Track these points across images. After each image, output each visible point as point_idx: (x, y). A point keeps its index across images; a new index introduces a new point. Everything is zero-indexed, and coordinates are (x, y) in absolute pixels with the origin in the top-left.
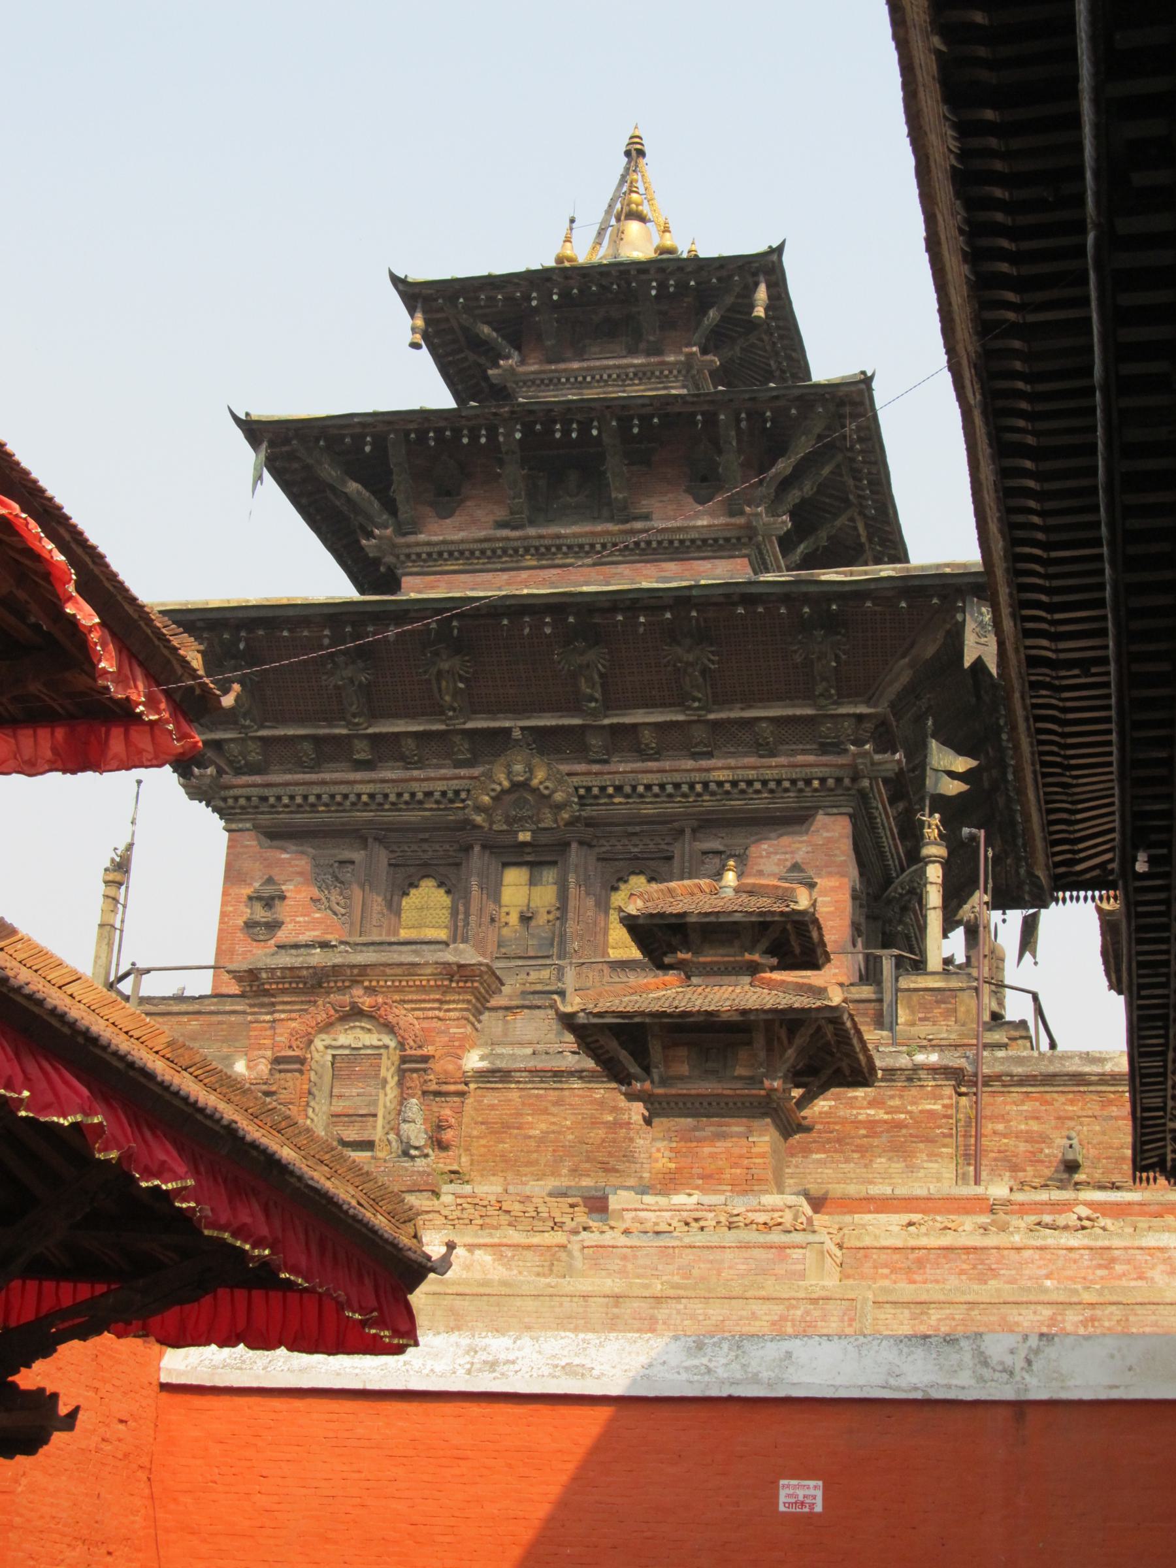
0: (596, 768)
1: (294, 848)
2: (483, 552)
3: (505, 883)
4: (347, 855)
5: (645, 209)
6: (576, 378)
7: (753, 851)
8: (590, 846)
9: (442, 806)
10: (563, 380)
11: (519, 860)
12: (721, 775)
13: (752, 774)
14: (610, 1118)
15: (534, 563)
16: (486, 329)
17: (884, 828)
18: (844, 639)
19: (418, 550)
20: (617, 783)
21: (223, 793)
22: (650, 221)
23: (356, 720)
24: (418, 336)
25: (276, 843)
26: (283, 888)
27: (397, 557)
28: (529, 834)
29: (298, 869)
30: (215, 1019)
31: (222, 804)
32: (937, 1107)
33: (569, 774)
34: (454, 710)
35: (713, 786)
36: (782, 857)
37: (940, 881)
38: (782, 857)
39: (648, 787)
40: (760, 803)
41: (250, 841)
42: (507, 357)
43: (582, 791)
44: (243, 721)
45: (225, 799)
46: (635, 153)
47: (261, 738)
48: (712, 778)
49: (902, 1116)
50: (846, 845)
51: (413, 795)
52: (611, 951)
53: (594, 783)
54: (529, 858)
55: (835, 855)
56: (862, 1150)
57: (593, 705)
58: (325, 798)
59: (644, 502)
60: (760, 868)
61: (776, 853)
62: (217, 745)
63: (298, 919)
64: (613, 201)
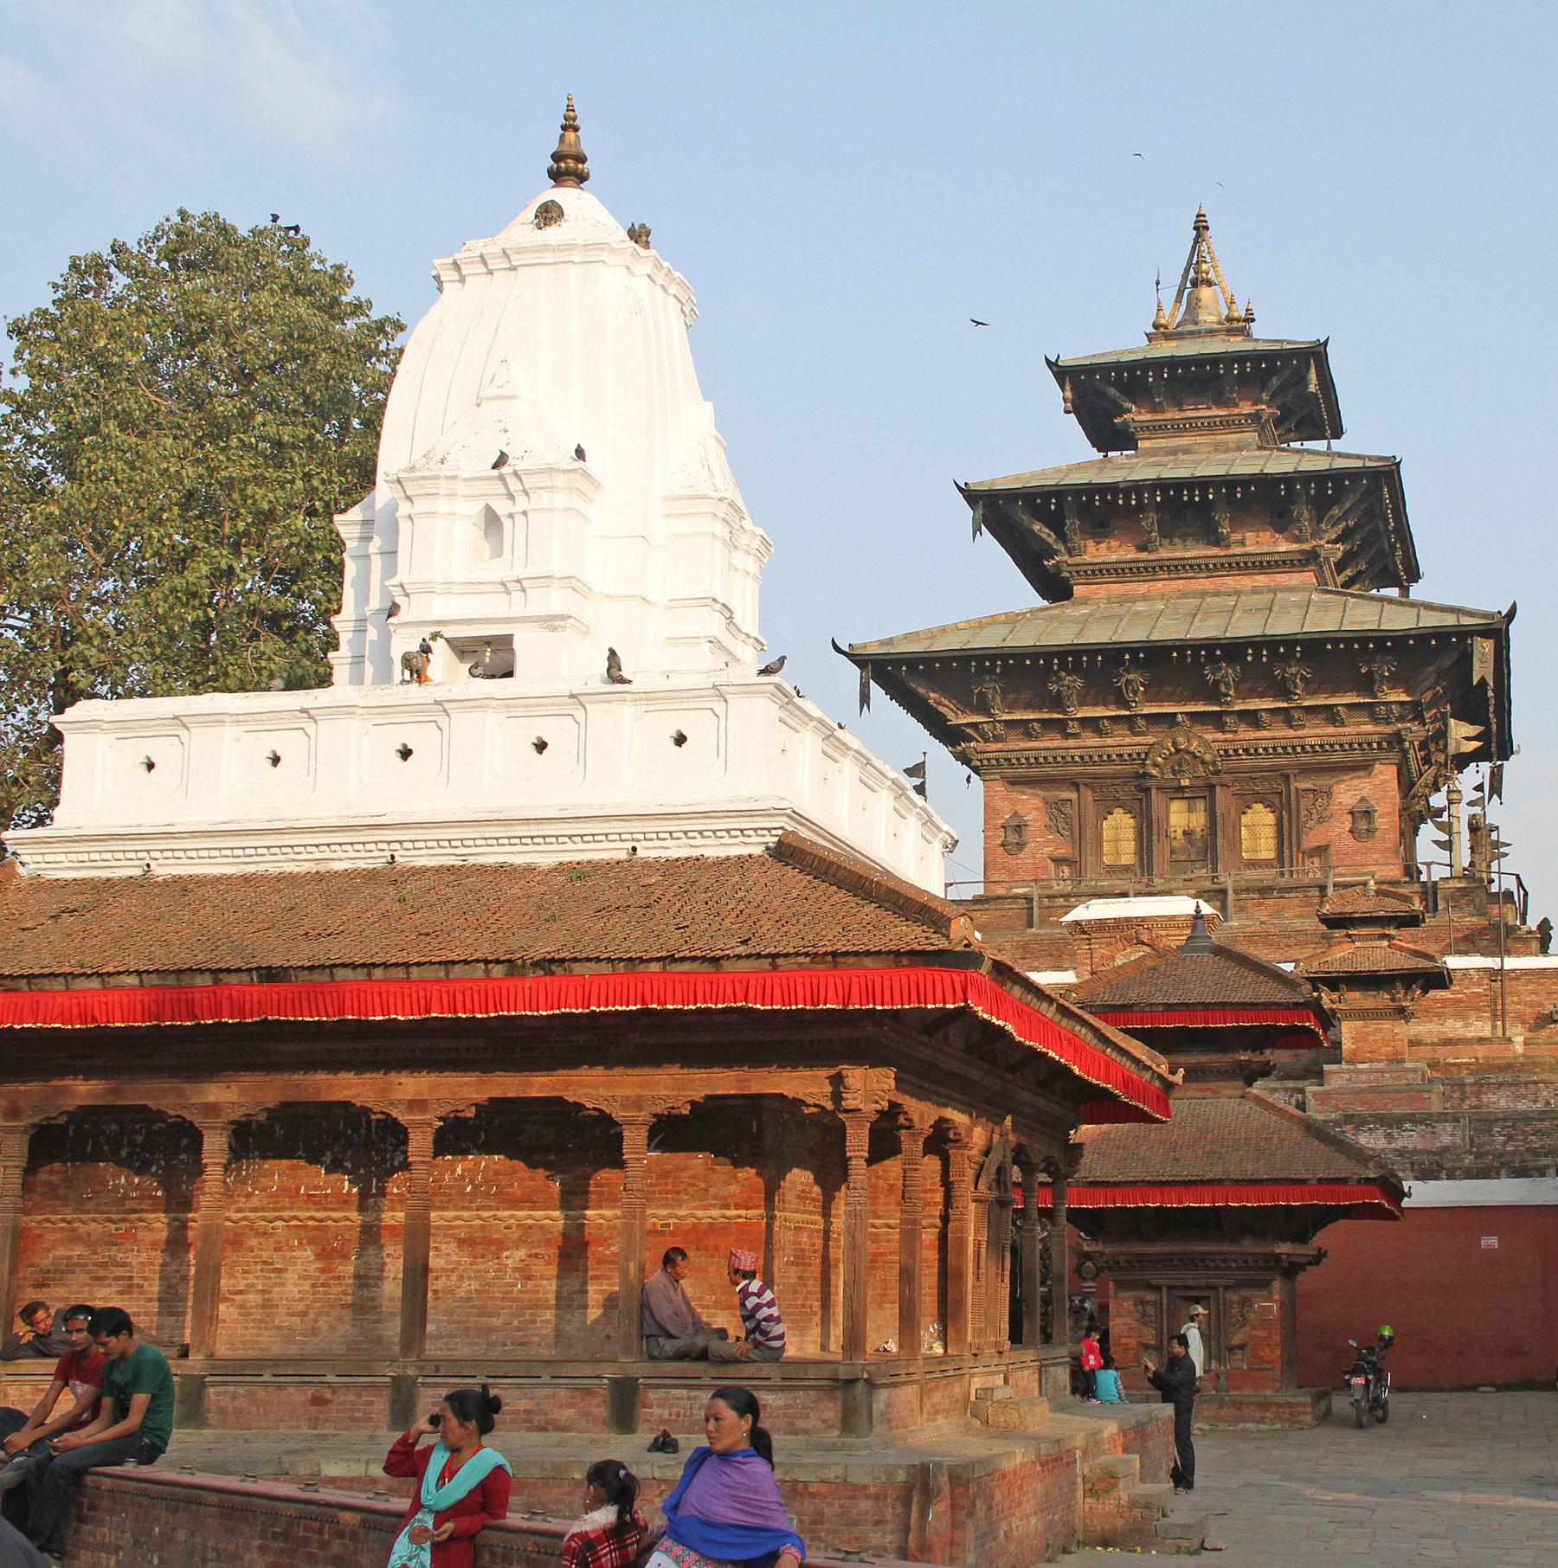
0: (1230, 736)
4: (1065, 795)
5: (1212, 276)
7: (1335, 789)
12: (1313, 741)
19: (1085, 568)
24: (1069, 405)
25: (1018, 788)
30: (998, 913)
39: (1265, 749)
40: (1336, 758)
41: (999, 788)
42: (1129, 411)
43: (1222, 753)
45: (981, 761)
46: (1201, 227)
47: (1005, 721)
51: (1109, 756)
56: (1438, 1015)
62: (974, 726)
64: (1187, 271)
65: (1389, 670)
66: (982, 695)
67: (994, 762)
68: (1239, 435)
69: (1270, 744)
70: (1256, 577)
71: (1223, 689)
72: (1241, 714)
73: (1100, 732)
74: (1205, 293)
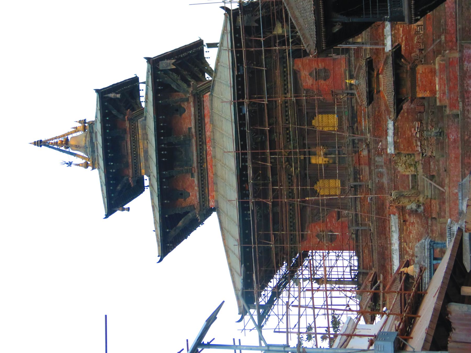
2: (202, 181)
6: (135, 157)
10: (135, 161)
14: (406, 114)
15: (205, 164)
16: (119, 188)
19: (202, 202)
27: (204, 209)
31: (293, 253)
32: (401, 29)
36: (307, 79)
38: (307, 79)
49: (404, 38)
51: (290, 192)
57: (263, 137)
58: (291, 220)
59: (185, 130)
60: (311, 85)
61: (306, 80)
68: (140, 129)
74: (71, 142)
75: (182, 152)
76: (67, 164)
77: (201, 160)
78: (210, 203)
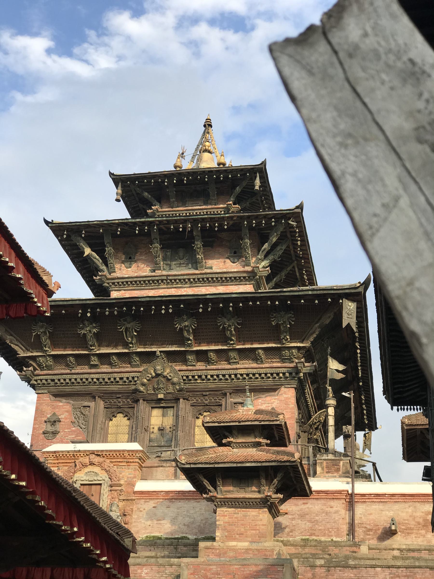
1: (64, 401)
3: (152, 415)
4: (86, 404)
5: (211, 149)
8: (187, 400)
9: (126, 383)
11: (158, 405)
13: (255, 371)
15: (165, 286)
16: (146, 194)
17: (309, 395)
18: (293, 316)
20: (199, 374)
21: (36, 378)
22: (213, 153)
23: (92, 348)
25: (57, 399)
26: (60, 417)
28: (162, 395)
29: (66, 410)
31: (35, 383)
33: (179, 371)
34: (132, 344)
35: (239, 376)
36: (267, 405)
37: (333, 414)
38: (267, 405)
39: (212, 376)
41: (47, 398)
43: (185, 378)
44: (45, 349)
45: (36, 381)
48: (238, 373)
50: (293, 400)
51: (115, 379)
52: (196, 444)
53: (190, 374)
54: (162, 405)
55: (289, 405)
59: (210, 262)
61: (265, 404)
62: (34, 358)
63: (65, 430)
65: (290, 324)
66: (38, 337)
67: (44, 381)
69: (215, 372)
70: (218, 287)
71: (186, 334)
72: (198, 353)
73: (111, 364)
75: (183, 259)
76: (183, 154)
77: (171, 280)
78: (116, 292)
